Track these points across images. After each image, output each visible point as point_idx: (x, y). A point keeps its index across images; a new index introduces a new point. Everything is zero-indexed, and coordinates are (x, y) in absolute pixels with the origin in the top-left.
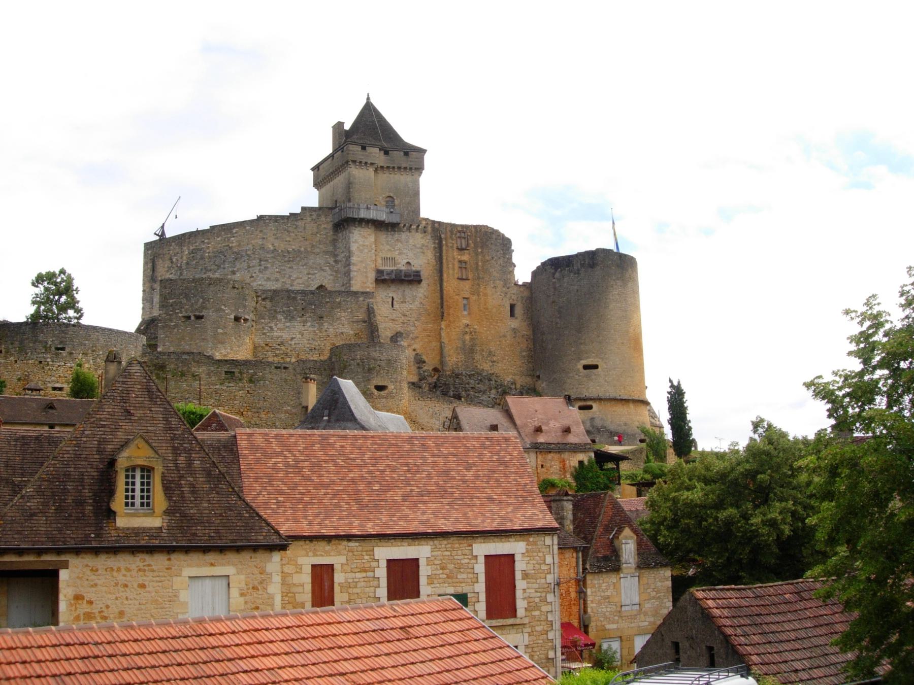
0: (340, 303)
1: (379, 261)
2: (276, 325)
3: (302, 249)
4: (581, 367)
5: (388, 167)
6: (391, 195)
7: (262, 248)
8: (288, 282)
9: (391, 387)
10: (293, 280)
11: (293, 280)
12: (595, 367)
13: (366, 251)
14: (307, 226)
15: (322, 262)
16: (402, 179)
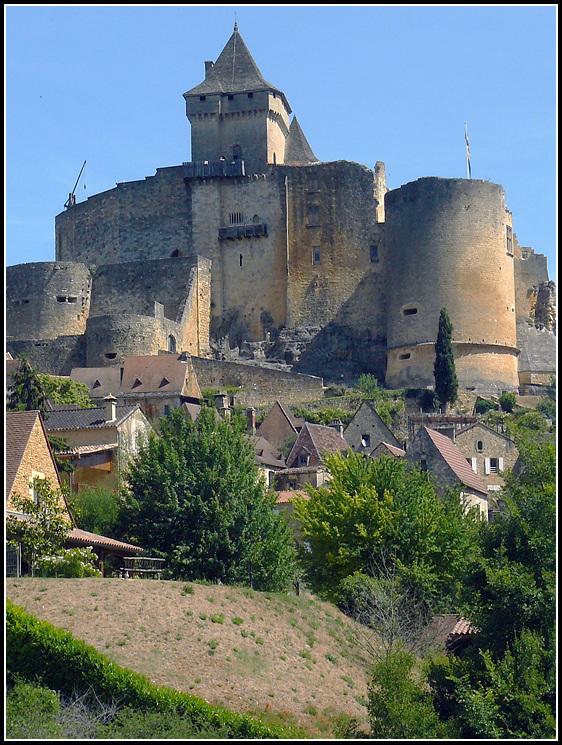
0: (165, 271)
1: (227, 218)
2: (111, 299)
3: (158, 214)
4: (402, 312)
5: (233, 114)
6: (238, 143)
7: (122, 217)
8: (146, 250)
9: (120, 354)
10: (150, 248)
11: (150, 248)
12: (414, 311)
13: (209, 209)
14: (162, 188)
15: (174, 224)
16: (247, 123)
